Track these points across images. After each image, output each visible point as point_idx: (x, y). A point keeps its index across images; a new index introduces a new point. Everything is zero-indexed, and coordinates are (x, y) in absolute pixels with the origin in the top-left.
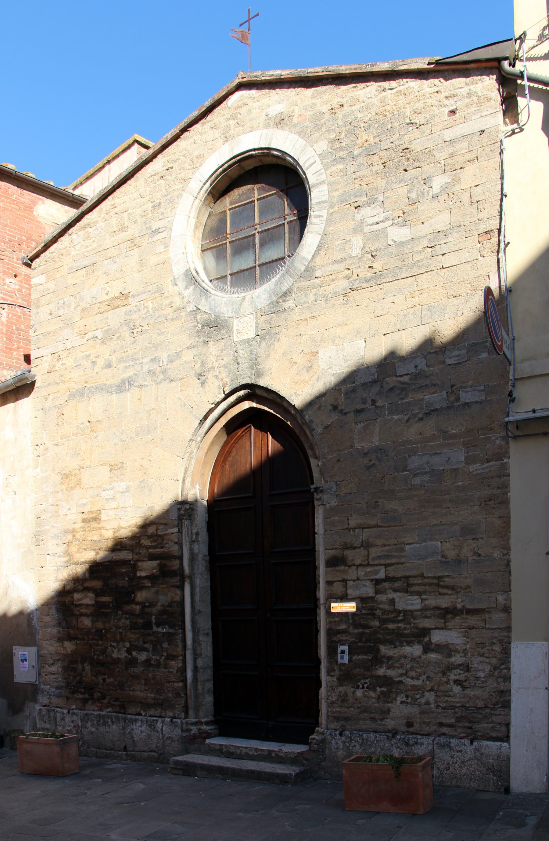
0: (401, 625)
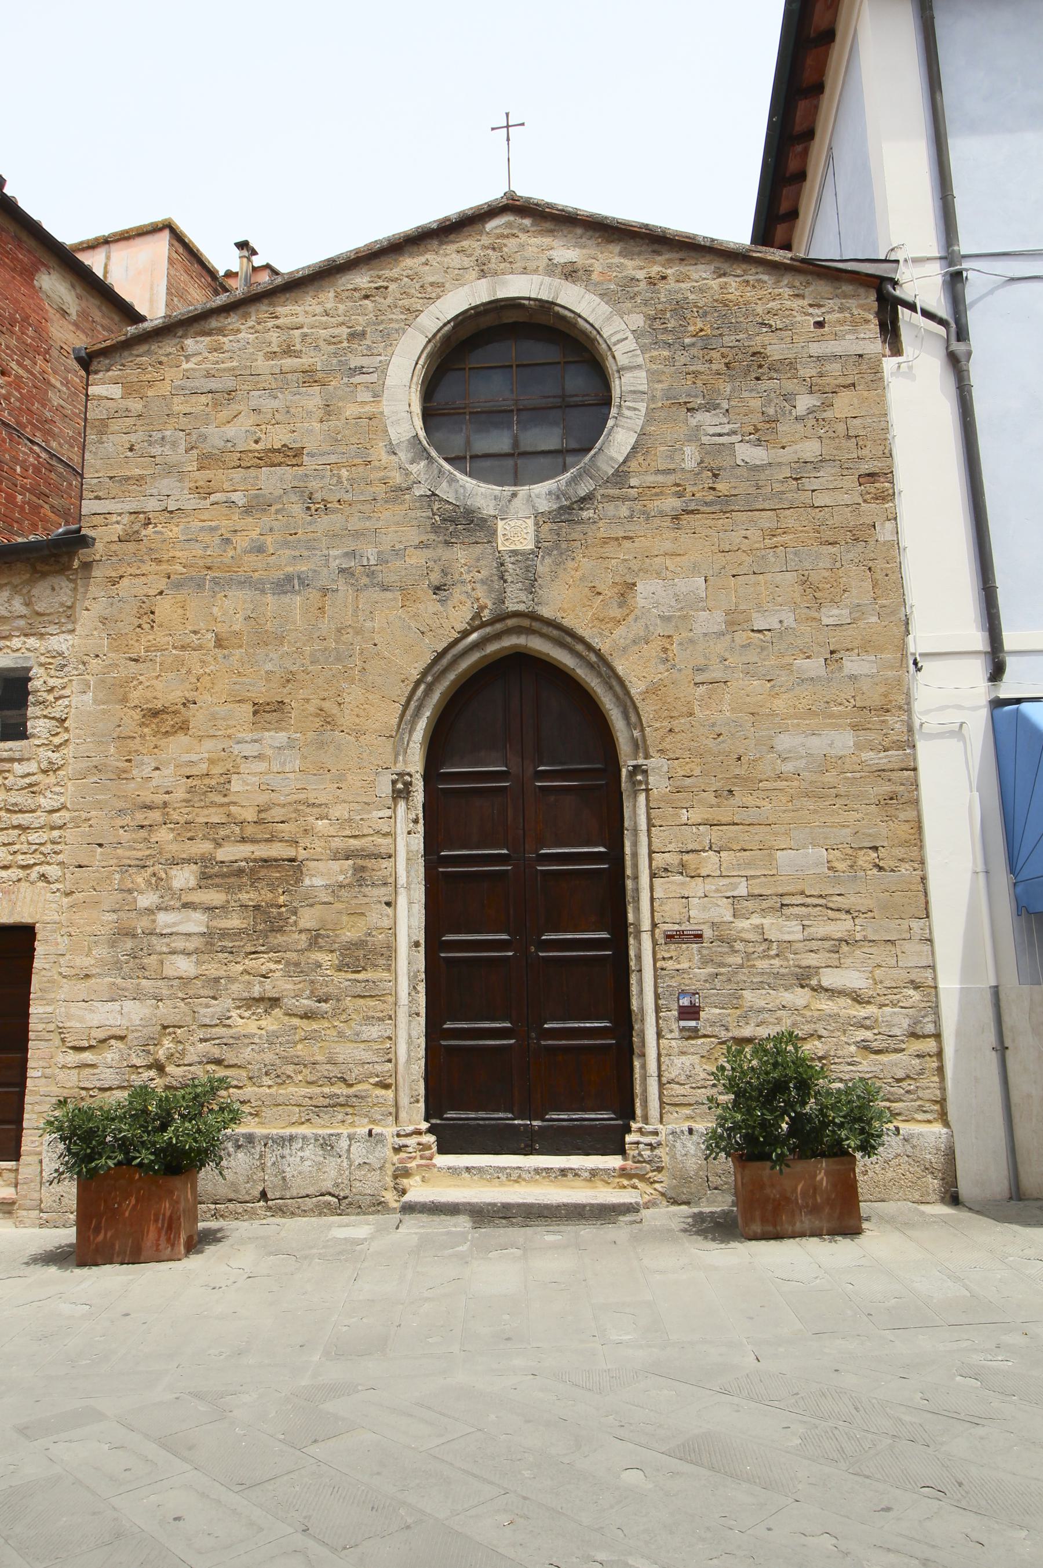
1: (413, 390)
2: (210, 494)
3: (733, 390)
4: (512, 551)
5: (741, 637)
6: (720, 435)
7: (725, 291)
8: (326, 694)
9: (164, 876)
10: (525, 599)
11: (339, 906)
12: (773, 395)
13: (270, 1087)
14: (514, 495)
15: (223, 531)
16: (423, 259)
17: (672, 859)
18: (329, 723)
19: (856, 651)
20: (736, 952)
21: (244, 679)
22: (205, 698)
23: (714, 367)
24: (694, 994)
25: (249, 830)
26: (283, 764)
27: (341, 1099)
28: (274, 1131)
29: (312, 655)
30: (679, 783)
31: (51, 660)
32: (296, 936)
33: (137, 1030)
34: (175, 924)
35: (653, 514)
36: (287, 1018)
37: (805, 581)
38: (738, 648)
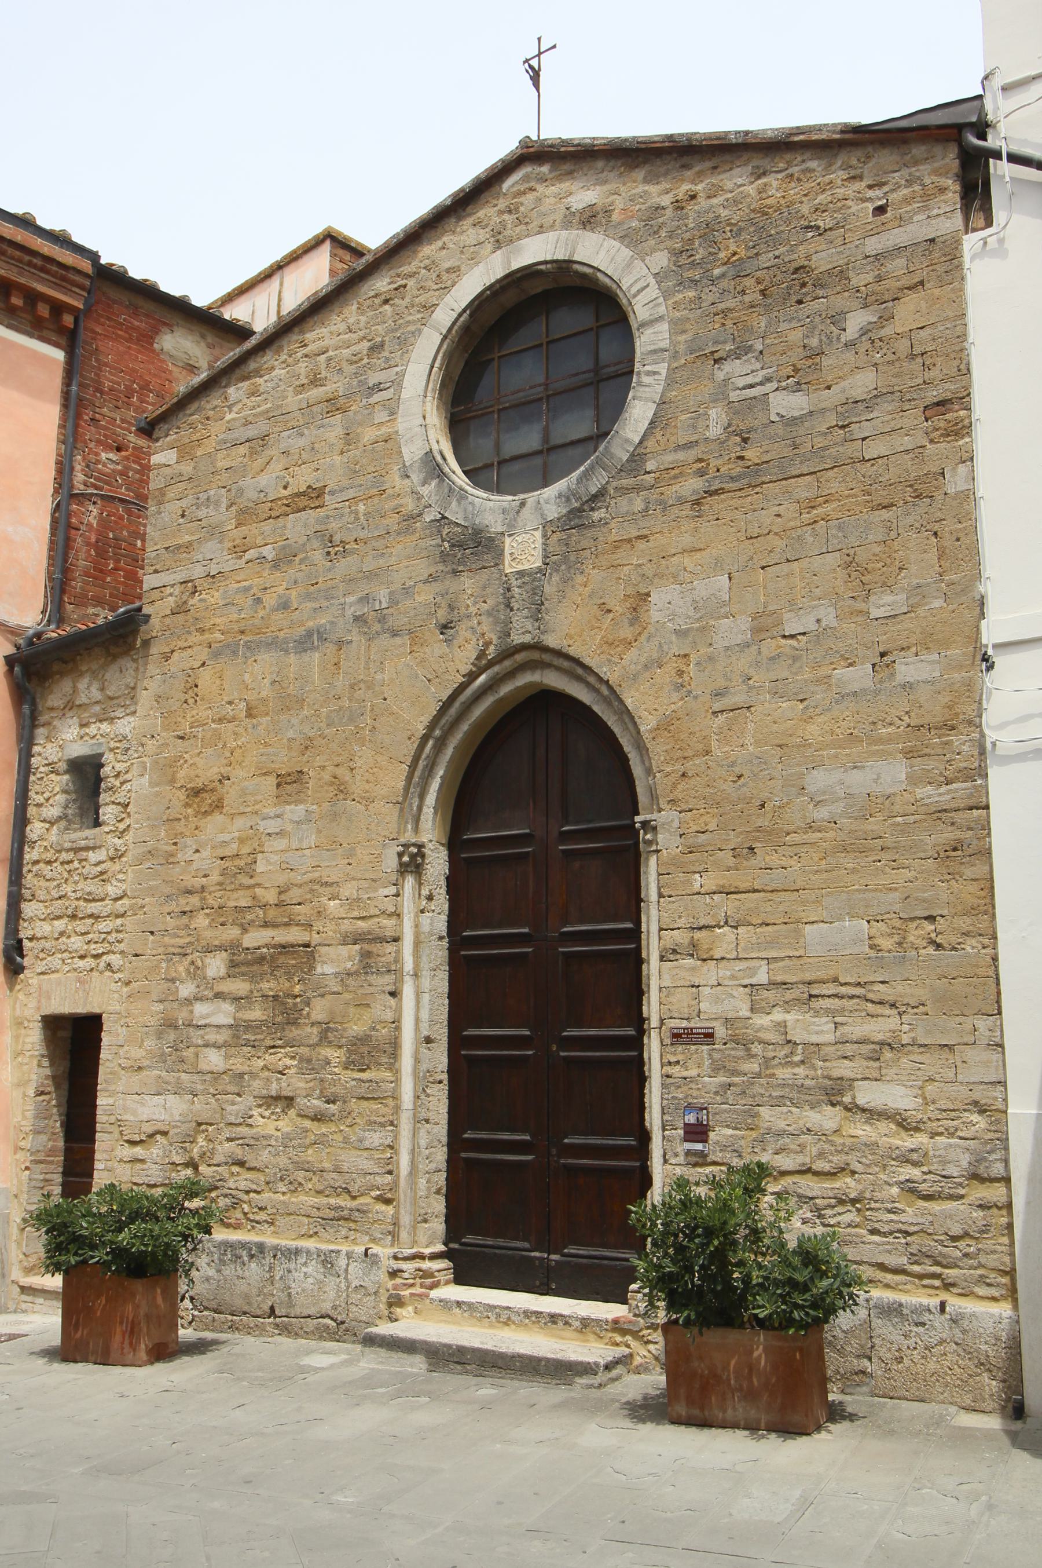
0: (801, 1071)
1: (429, 398)
2: (245, 552)
3: (769, 324)
4: (518, 573)
5: (769, 647)
6: (752, 386)
7: (764, 195)
8: (339, 760)
9: (200, 964)
10: (530, 629)
11: (347, 996)
12: (817, 319)
13: (284, 1193)
14: (523, 504)
15: (255, 590)
16: (440, 243)
17: (680, 937)
18: (341, 791)
19: (913, 650)
20: (754, 1056)
21: (270, 750)
22: (238, 773)
23: (747, 299)
24: (702, 1109)
25: (272, 913)
26: (301, 840)
27: (345, 1212)
28: (283, 1242)
29: (328, 717)
30: (691, 841)
31: (118, 745)
32: (308, 1029)
33: (177, 1127)
34: (208, 1016)
35: (671, 502)
36: (300, 1119)
37: (850, 563)
38: (765, 661)
